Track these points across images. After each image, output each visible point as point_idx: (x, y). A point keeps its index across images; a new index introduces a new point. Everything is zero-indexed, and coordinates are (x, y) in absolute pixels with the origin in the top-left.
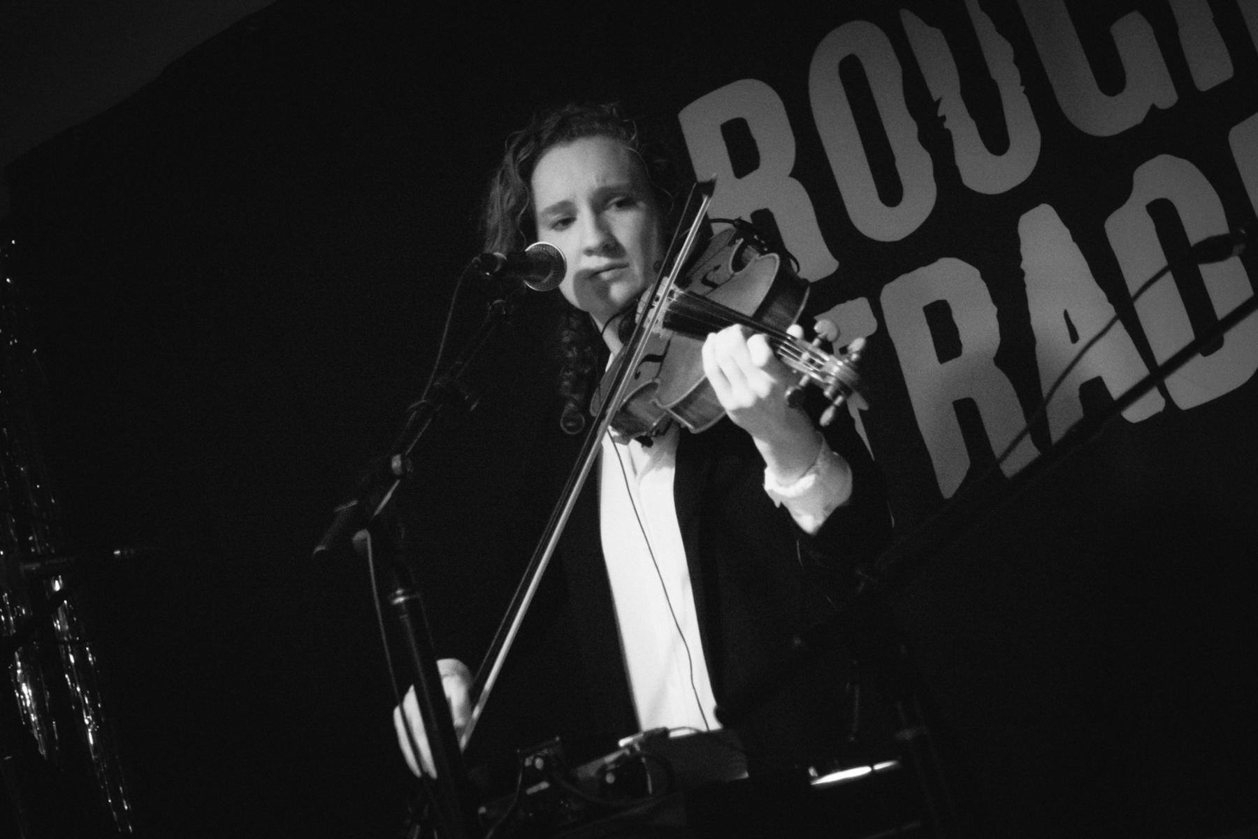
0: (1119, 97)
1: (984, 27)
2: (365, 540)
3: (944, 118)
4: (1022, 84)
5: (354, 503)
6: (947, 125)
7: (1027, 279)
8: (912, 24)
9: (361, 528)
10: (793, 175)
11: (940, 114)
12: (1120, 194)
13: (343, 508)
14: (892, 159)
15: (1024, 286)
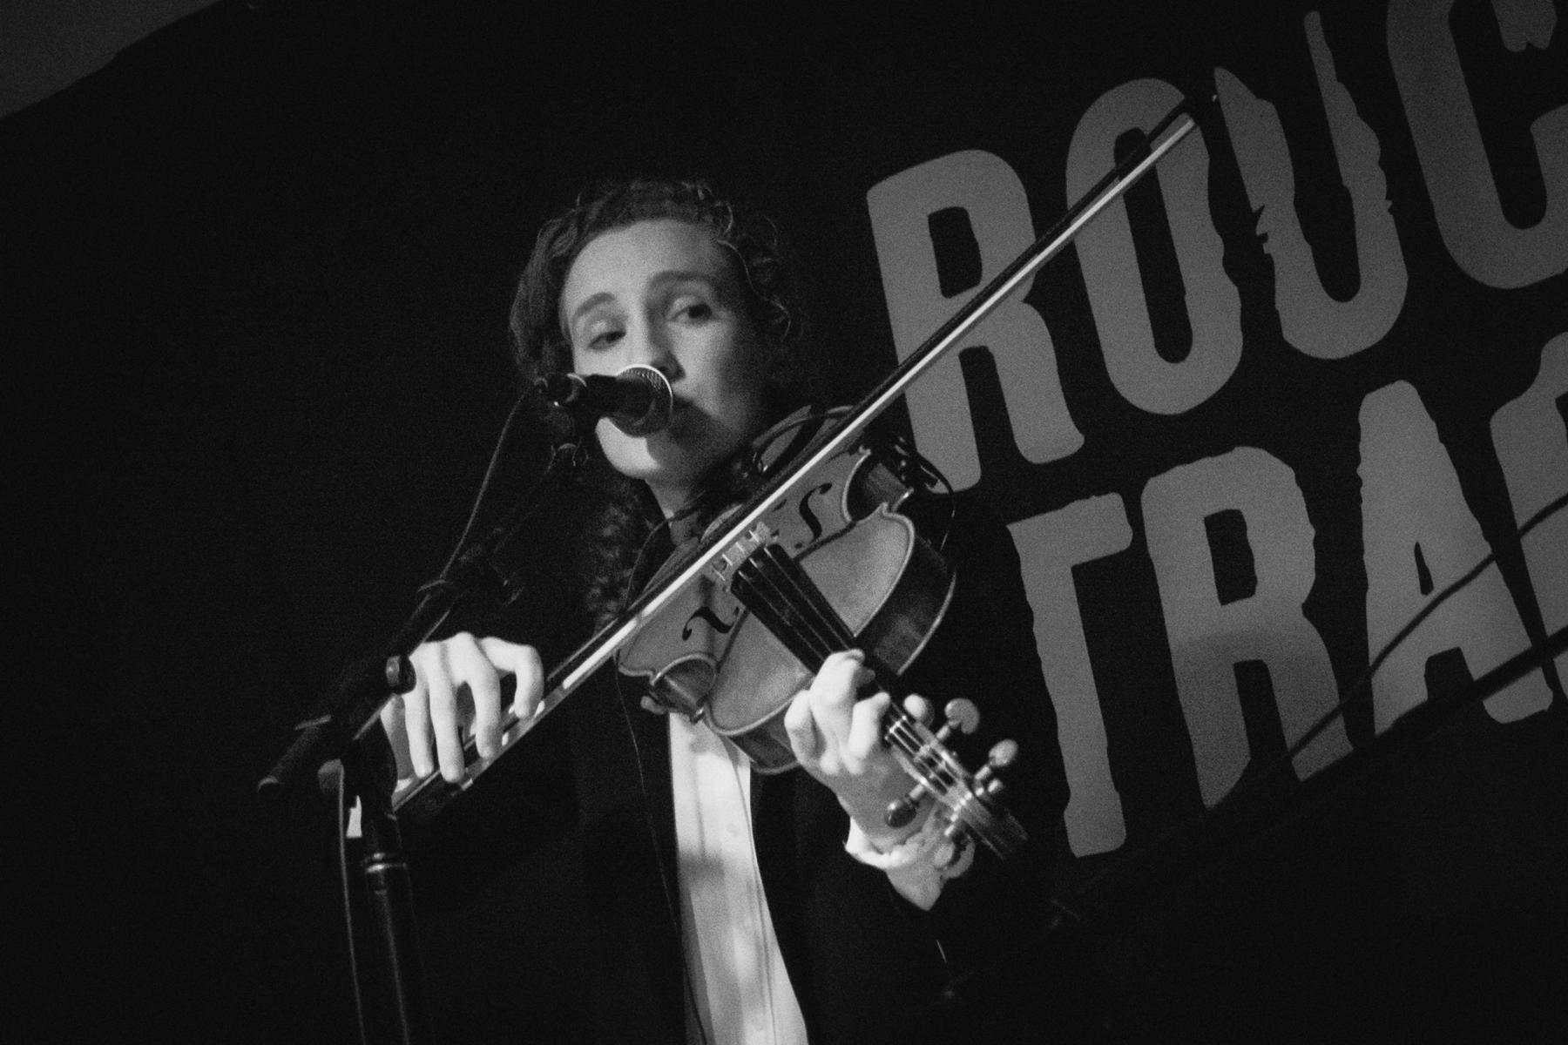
0: (1530, 234)
1: (1339, 104)
2: (336, 774)
3: (1264, 237)
4: (1388, 198)
5: (325, 720)
6: (1267, 248)
7: (1364, 492)
8: (1229, 89)
9: (333, 758)
10: (1027, 300)
11: (1259, 231)
12: (1519, 378)
13: (309, 725)
14: (1180, 290)
15: (1360, 500)
